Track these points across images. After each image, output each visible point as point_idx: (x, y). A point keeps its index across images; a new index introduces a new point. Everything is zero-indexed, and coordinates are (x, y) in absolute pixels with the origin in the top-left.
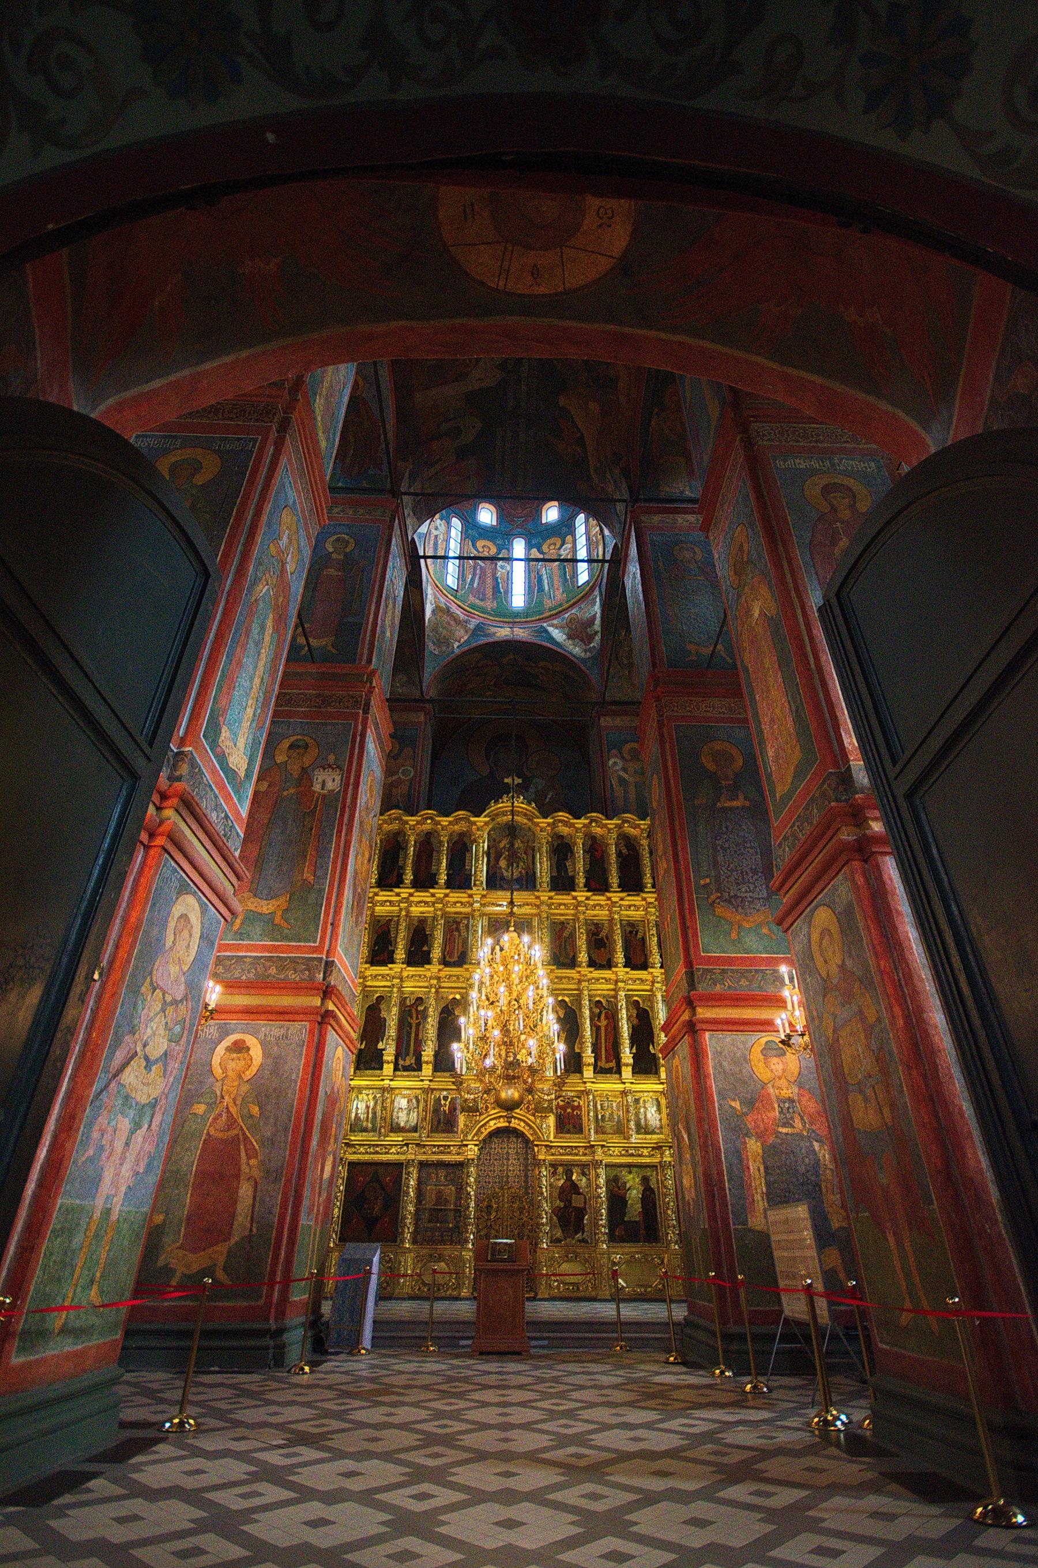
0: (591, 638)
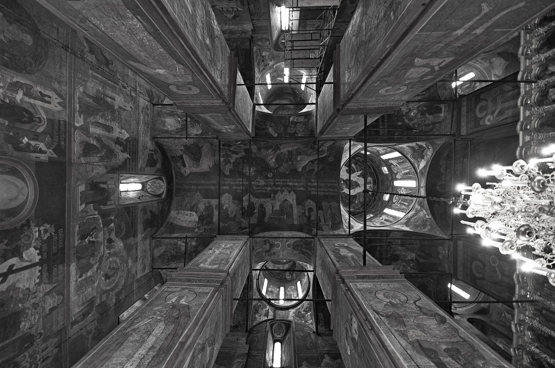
0: (421, 147)
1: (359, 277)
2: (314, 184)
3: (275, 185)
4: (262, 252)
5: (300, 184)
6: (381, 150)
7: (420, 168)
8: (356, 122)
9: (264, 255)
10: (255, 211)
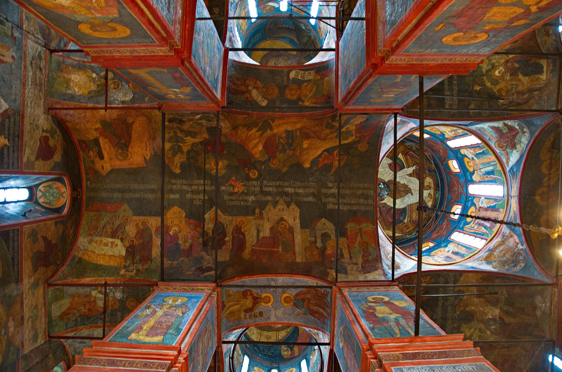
0: (511, 129)
1: (406, 356)
2: (332, 191)
3: (263, 193)
4: (239, 311)
5: (307, 190)
6: (447, 131)
7: (511, 164)
8: (405, 86)
9: (242, 316)
10: (227, 239)
